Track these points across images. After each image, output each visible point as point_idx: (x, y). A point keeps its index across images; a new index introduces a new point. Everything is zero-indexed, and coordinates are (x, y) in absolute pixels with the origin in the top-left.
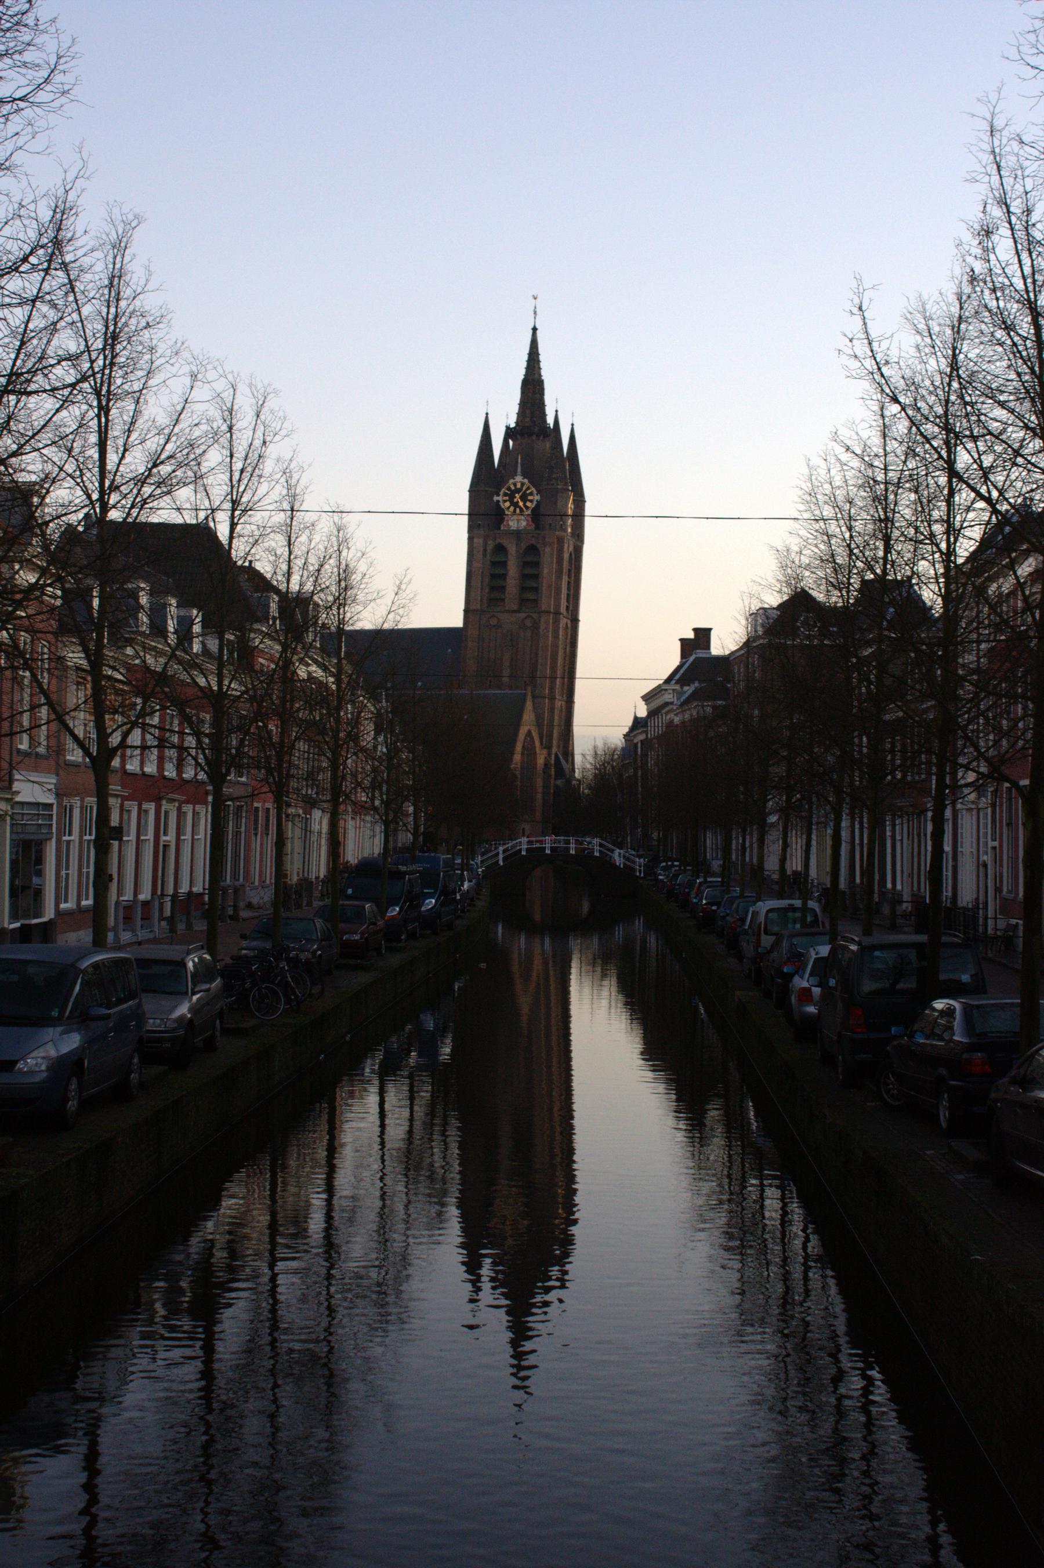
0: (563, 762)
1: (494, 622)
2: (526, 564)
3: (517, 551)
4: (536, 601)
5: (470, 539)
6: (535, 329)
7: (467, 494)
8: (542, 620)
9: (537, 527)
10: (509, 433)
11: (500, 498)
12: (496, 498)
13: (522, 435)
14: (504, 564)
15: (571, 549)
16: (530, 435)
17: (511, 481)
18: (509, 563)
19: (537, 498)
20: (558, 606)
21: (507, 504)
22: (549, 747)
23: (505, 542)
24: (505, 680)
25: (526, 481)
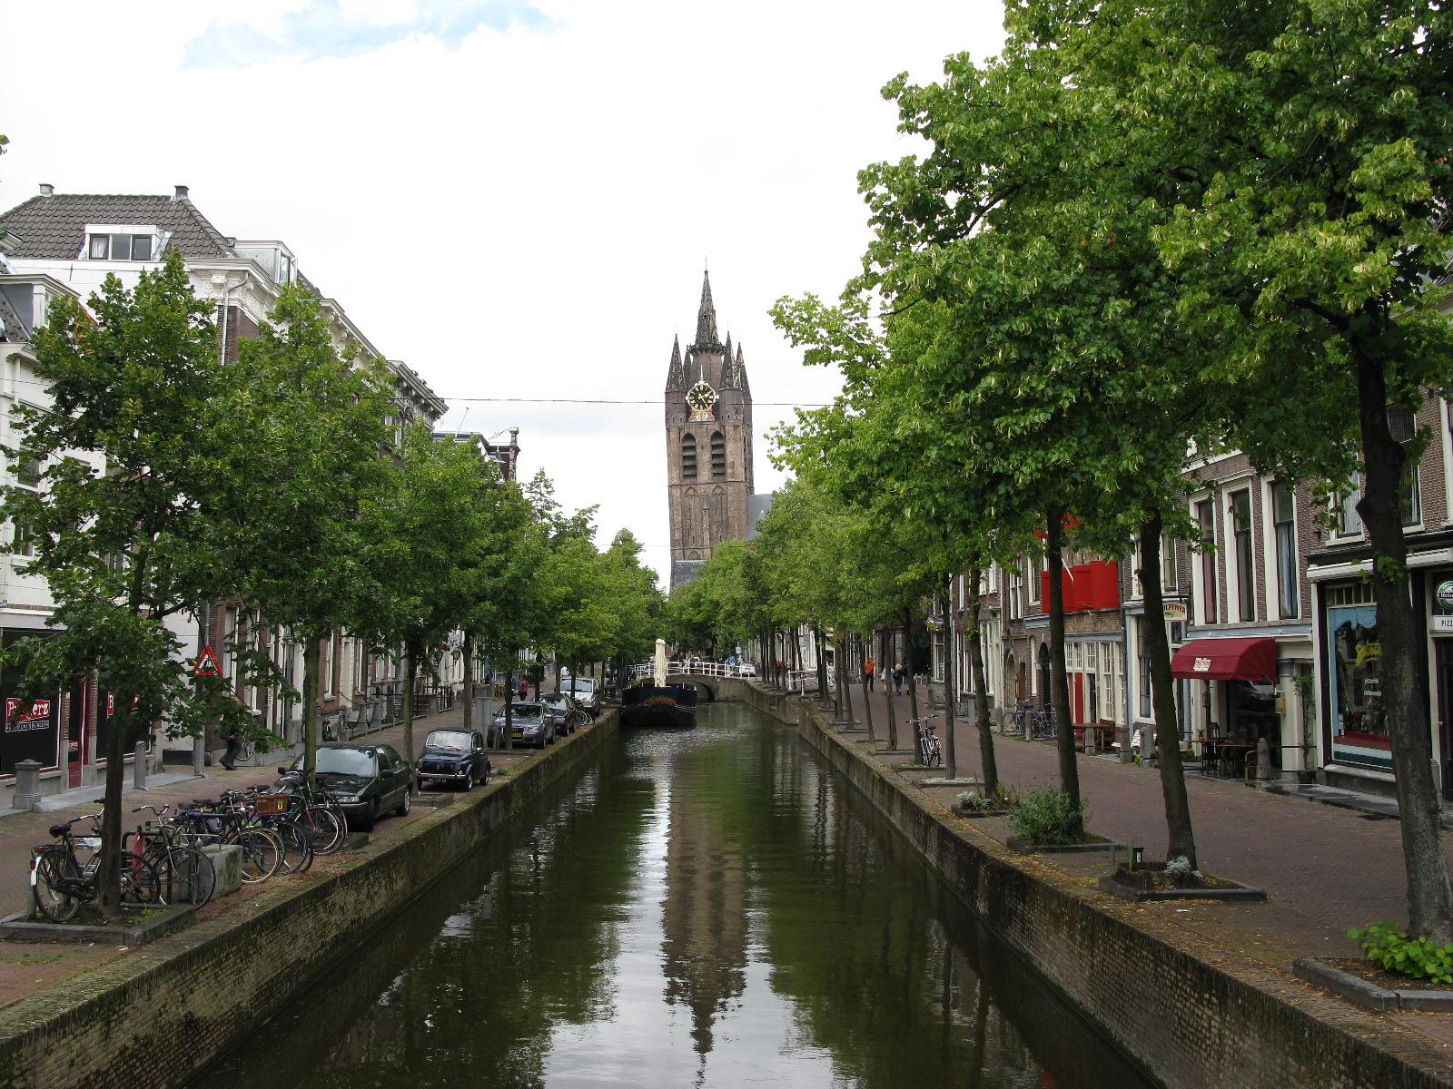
6: (706, 272)
16: (707, 351)
23: (693, 432)
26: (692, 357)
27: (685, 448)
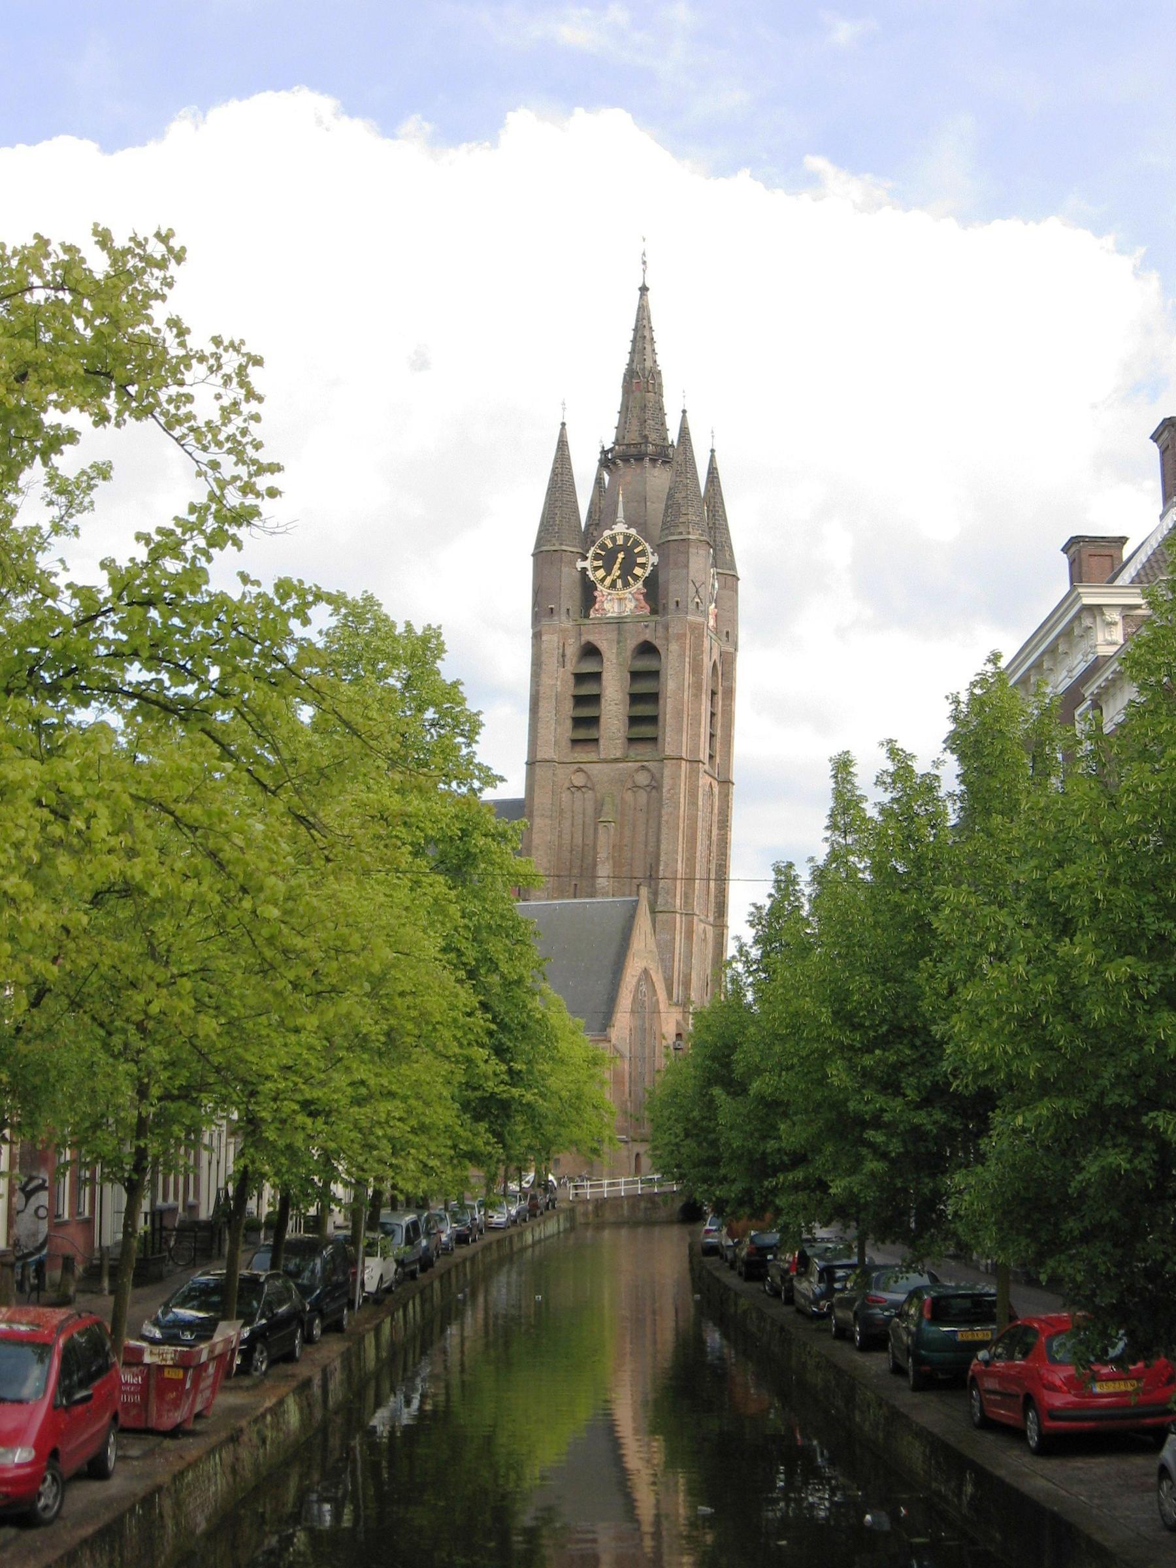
1: (579, 780)
2: (636, 675)
3: (619, 654)
4: (654, 740)
5: (537, 636)
6: (644, 289)
7: (529, 562)
8: (667, 772)
9: (654, 611)
10: (607, 461)
11: (587, 564)
12: (580, 564)
13: (626, 459)
14: (596, 677)
15: (715, 656)
16: (639, 458)
17: (607, 533)
18: (605, 676)
19: (654, 559)
20: (696, 749)
21: (601, 573)
24: (602, 882)
25: (633, 531)
26: (607, 477)
27: (580, 678)
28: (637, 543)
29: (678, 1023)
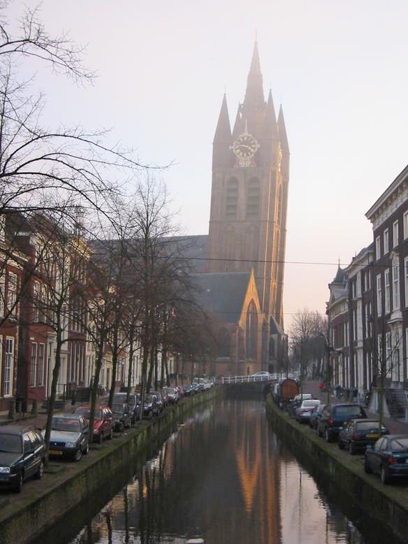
0: (276, 323)
11: (233, 147)
14: (236, 190)
15: (281, 183)
17: (241, 136)
19: (258, 146)
22: (267, 313)
28: (252, 140)
29: (264, 320)
